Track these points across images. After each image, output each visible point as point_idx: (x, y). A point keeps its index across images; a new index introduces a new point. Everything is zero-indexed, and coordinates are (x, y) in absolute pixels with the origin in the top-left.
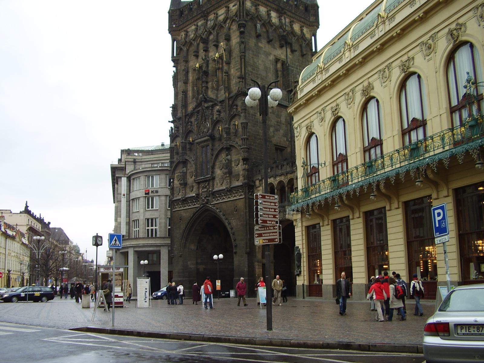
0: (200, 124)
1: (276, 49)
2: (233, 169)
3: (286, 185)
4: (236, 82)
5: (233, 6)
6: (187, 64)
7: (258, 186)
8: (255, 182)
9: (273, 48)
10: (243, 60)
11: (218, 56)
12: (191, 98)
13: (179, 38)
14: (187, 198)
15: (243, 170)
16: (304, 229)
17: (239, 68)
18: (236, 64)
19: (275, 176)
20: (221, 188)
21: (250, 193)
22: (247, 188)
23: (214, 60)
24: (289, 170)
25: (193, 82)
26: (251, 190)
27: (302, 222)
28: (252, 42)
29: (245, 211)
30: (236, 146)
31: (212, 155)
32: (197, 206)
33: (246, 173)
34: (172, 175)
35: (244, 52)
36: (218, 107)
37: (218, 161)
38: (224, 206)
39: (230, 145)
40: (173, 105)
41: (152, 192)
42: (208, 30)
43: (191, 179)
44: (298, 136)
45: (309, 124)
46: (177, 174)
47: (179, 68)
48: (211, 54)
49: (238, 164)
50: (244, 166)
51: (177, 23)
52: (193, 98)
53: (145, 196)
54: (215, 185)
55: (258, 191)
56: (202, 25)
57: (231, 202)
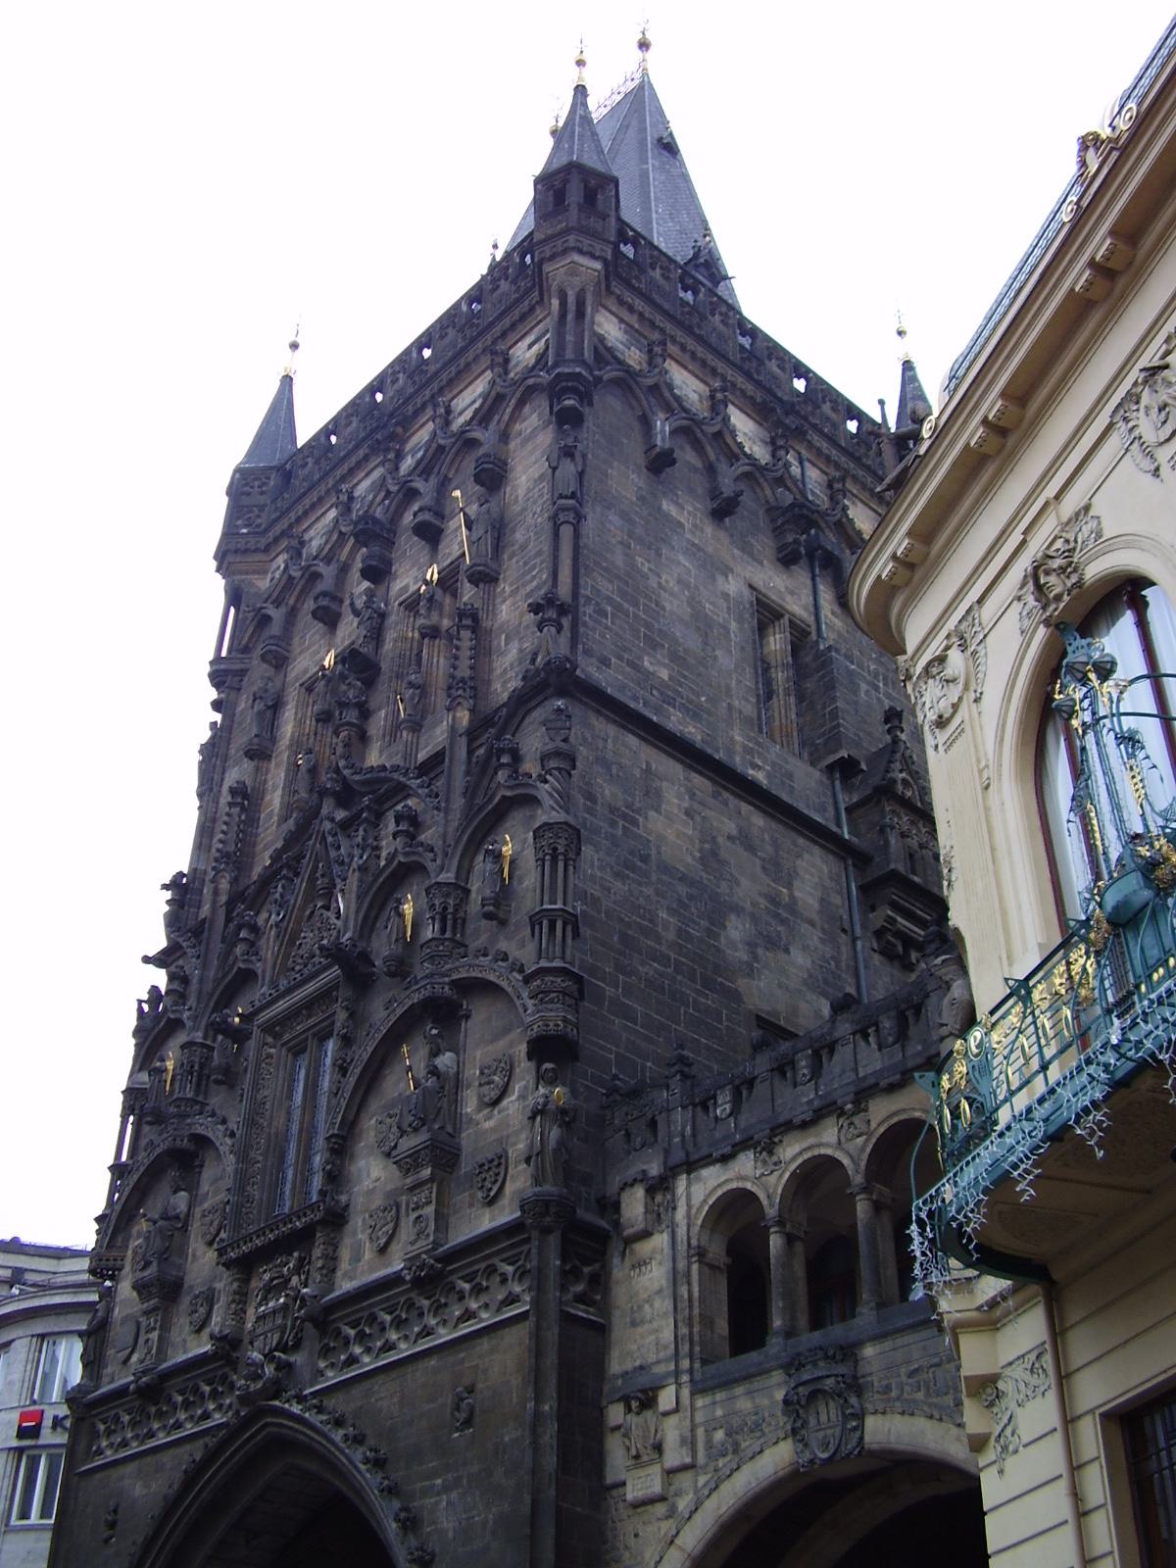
0: (298, 922)
1: (761, 563)
2: (466, 1138)
3: (858, 1179)
4: (521, 651)
5: (530, 346)
6: (281, 676)
7: (640, 1226)
8: (616, 1206)
9: (743, 550)
10: (566, 532)
11: (436, 576)
12: (276, 818)
15: (532, 1118)
16: (1091, 1438)
18: (524, 575)
19: (765, 1144)
21: (579, 1288)
22: (554, 1240)
24: (878, 1066)
25: (296, 745)
26: (587, 1263)
28: (626, 481)
29: (531, 1405)
30: (492, 977)
32: (218, 1418)
33: (555, 1133)
34: (110, 1246)
35: (573, 496)
37: (375, 1104)
39: (454, 984)
44: (955, 707)
49: (504, 1092)
50: (542, 1090)
51: (259, 521)
53: (15, 1443)
54: (344, 1265)
55: (640, 1264)
57: (433, 1362)
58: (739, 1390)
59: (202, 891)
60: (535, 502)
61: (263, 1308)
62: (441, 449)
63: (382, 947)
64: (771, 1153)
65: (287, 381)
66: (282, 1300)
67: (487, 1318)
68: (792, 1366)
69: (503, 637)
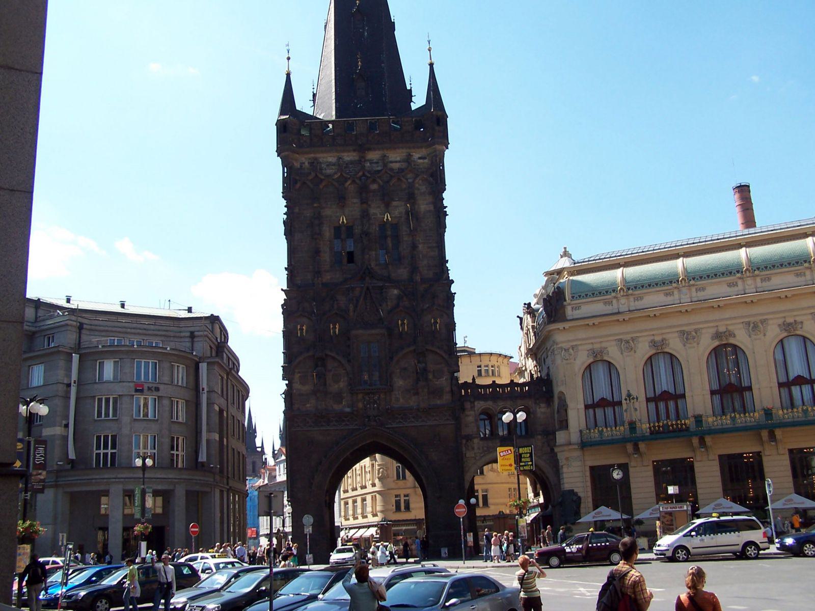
5: (420, 158)
13: (295, 164)
16: (588, 469)
27: (584, 461)
31: (391, 358)
32: (351, 427)
36: (396, 292)
40: (288, 265)
41: (149, 389)
42: (369, 175)
43: (336, 386)
44: (570, 359)
46: (299, 375)
47: (297, 210)
55: (468, 416)
56: (352, 162)
61: (368, 406)
65: (288, 75)
66: (376, 406)
69: (421, 256)
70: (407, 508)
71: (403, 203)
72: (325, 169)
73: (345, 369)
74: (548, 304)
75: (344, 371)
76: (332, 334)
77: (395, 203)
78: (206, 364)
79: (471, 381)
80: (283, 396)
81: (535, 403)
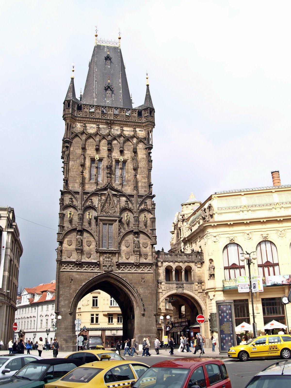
5: (140, 131)
11: (122, 159)
14: (83, 262)
17: (146, 177)
18: (141, 173)
20: (127, 261)
23: (117, 161)
30: (146, 233)
32: (96, 271)
36: (123, 199)
38: (130, 276)
43: (88, 247)
45: (233, 238)
46: (68, 239)
47: (71, 149)
48: (116, 154)
49: (147, 247)
52: (90, 181)
56: (104, 128)
57: (138, 274)
58: (170, 284)
59: (68, 182)
60: (142, 162)
62: (122, 135)
63: (124, 219)
64: (174, 263)
65: (72, 79)
67: (146, 271)
68: (177, 284)
70: (97, 321)
71: (130, 152)
72: (89, 130)
73: (94, 238)
74: (204, 212)
75: (93, 239)
76: (87, 218)
77: (125, 152)
78: (6, 232)
79: (161, 251)
80: (57, 250)
81: (195, 265)
